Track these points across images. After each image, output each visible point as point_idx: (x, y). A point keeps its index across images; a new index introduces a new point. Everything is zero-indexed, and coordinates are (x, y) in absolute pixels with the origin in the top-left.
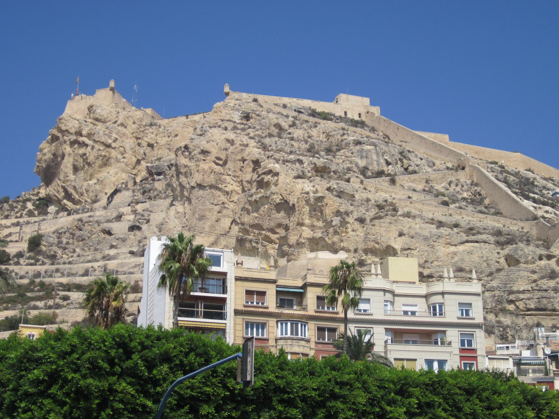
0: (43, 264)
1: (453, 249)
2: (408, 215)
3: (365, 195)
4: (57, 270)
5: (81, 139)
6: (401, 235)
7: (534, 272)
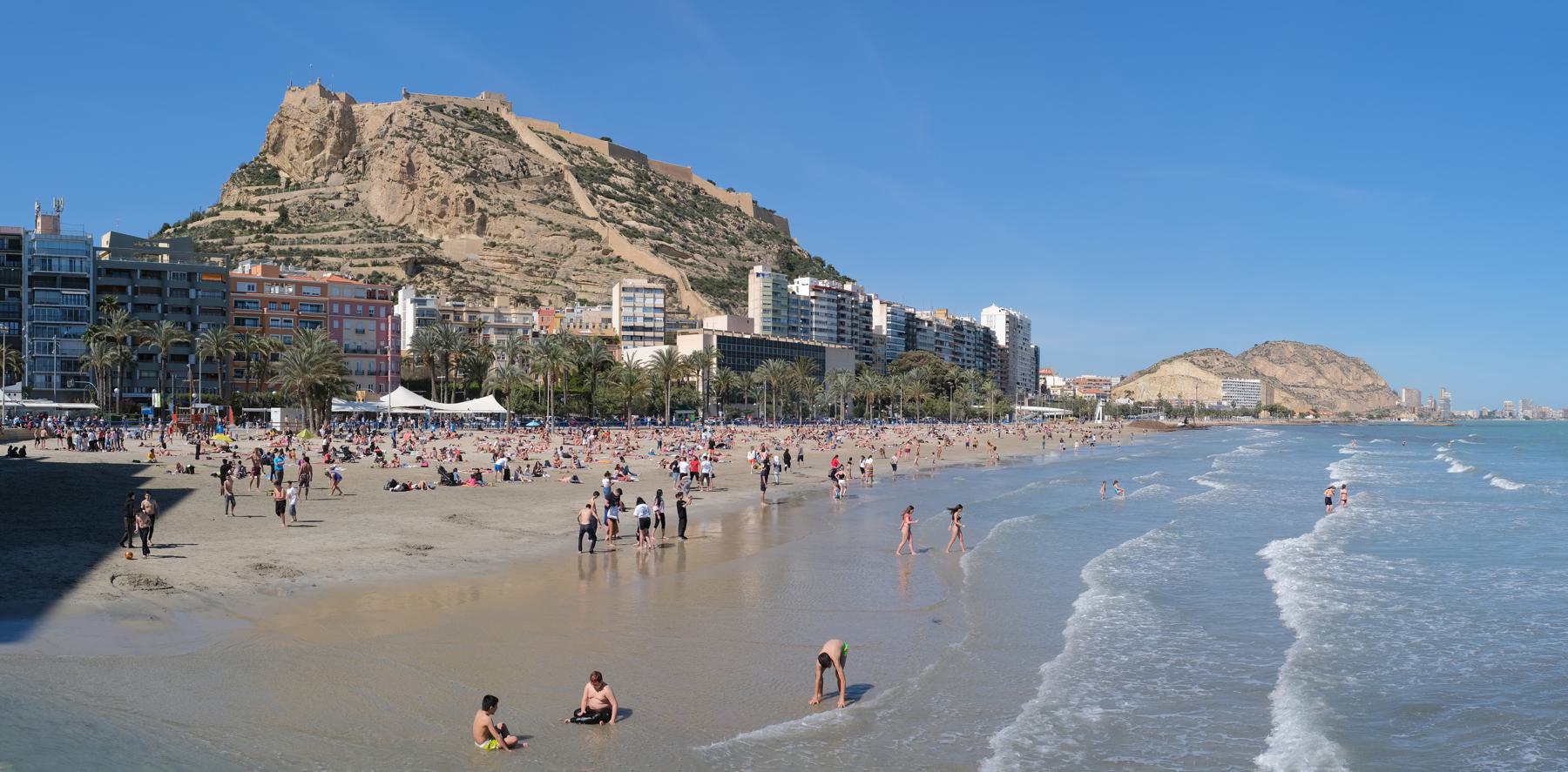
0: (293, 232)
1: (546, 239)
2: (523, 214)
3: (497, 196)
4: (304, 238)
5: (300, 126)
6: (517, 227)
7: (588, 259)
